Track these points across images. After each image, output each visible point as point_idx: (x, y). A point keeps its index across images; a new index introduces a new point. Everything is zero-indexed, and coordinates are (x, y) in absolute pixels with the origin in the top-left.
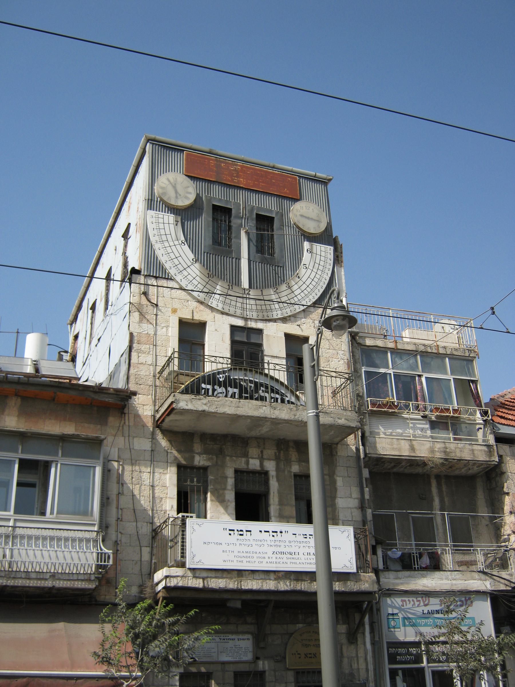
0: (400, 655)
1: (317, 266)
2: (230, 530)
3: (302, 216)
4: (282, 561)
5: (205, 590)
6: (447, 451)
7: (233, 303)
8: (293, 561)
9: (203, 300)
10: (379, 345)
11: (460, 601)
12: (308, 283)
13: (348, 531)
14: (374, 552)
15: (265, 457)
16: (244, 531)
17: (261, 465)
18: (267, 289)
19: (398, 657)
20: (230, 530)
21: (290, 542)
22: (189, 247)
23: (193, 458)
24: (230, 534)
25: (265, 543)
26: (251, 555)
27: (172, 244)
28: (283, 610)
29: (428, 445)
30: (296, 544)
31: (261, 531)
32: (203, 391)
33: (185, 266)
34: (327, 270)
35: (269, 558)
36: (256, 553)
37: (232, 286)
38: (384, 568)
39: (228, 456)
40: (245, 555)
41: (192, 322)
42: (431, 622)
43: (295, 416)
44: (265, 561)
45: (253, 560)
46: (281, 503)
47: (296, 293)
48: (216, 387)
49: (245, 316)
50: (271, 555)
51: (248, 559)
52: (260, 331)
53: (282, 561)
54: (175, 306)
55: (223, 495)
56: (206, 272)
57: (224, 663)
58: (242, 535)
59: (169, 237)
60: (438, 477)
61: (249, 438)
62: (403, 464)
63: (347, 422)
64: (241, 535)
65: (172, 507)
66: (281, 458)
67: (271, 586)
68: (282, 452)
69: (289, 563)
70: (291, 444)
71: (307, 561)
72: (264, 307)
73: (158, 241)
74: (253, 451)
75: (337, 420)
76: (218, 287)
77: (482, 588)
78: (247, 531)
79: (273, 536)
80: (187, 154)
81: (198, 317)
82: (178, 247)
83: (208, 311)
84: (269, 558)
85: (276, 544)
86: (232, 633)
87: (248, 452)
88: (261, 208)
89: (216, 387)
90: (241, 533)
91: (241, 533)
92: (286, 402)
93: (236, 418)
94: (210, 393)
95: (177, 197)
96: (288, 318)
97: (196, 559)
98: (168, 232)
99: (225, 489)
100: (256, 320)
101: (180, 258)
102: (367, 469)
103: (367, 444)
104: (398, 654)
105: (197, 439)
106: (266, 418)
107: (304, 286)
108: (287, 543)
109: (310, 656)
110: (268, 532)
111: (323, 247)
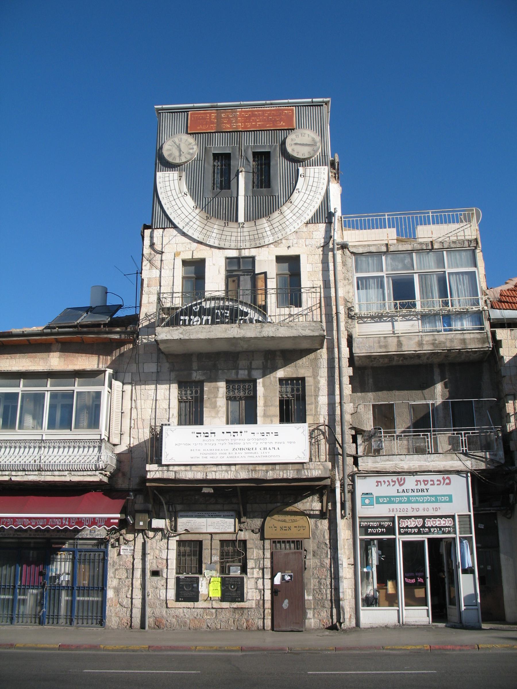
0: (373, 527)
1: (309, 187)
2: (197, 433)
3: (296, 144)
4: (240, 455)
5: (176, 481)
6: (435, 343)
7: (228, 238)
8: (251, 455)
9: (202, 241)
10: (372, 251)
11: (438, 480)
12: (299, 206)
13: (303, 428)
14: (355, 440)
15: (253, 367)
16: (209, 433)
17: (249, 374)
18: (260, 220)
19: (369, 530)
20: (197, 433)
21: (249, 440)
22: (191, 196)
23: (190, 375)
24: (197, 437)
25: (227, 442)
26: (214, 452)
27: (176, 197)
28: (264, 492)
29: (417, 339)
30: (254, 441)
31: (223, 433)
32: (181, 322)
33: (187, 214)
34: (320, 189)
35: (229, 453)
36: (219, 450)
37: (228, 223)
38: (364, 454)
39: (221, 369)
40: (209, 452)
41: (192, 260)
42: (405, 500)
43: (260, 332)
44: (226, 456)
45: (216, 456)
46: (266, 405)
47: (288, 217)
48: (192, 317)
49: (239, 248)
50: (231, 451)
51: (212, 456)
52: (253, 258)
53: (240, 455)
54: (179, 250)
55: (216, 402)
56: (204, 215)
57: (211, 534)
58: (208, 436)
59: (173, 192)
60: (441, 366)
61: (239, 353)
62: (396, 358)
63: (309, 331)
64: (206, 436)
65: (173, 415)
66: (269, 366)
67: (232, 475)
68: (269, 361)
69: (246, 457)
70: (278, 353)
71: (263, 455)
72: (256, 236)
73: (165, 197)
74: (242, 363)
75: (301, 331)
76: (216, 227)
77: (461, 467)
78: (211, 433)
79: (234, 436)
80: (191, 114)
81: (198, 255)
82: (181, 199)
83: (208, 248)
84: (229, 453)
85: (236, 442)
86: (219, 511)
87: (238, 365)
88: (257, 146)
89: (192, 317)
90: (207, 435)
91: (207, 435)
92: (254, 322)
93: (210, 341)
94: (187, 323)
95: (180, 155)
96: (280, 242)
97: (169, 457)
98: (172, 188)
99: (216, 397)
100: (249, 248)
101: (182, 209)
102: (351, 368)
103: (355, 345)
104: (369, 527)
105: (194, 359)
106: (234, 338)
107: (297, 209)
108: (246, 441)
109: (285, 528)
110: (230, 433)
111: (317, 168)
